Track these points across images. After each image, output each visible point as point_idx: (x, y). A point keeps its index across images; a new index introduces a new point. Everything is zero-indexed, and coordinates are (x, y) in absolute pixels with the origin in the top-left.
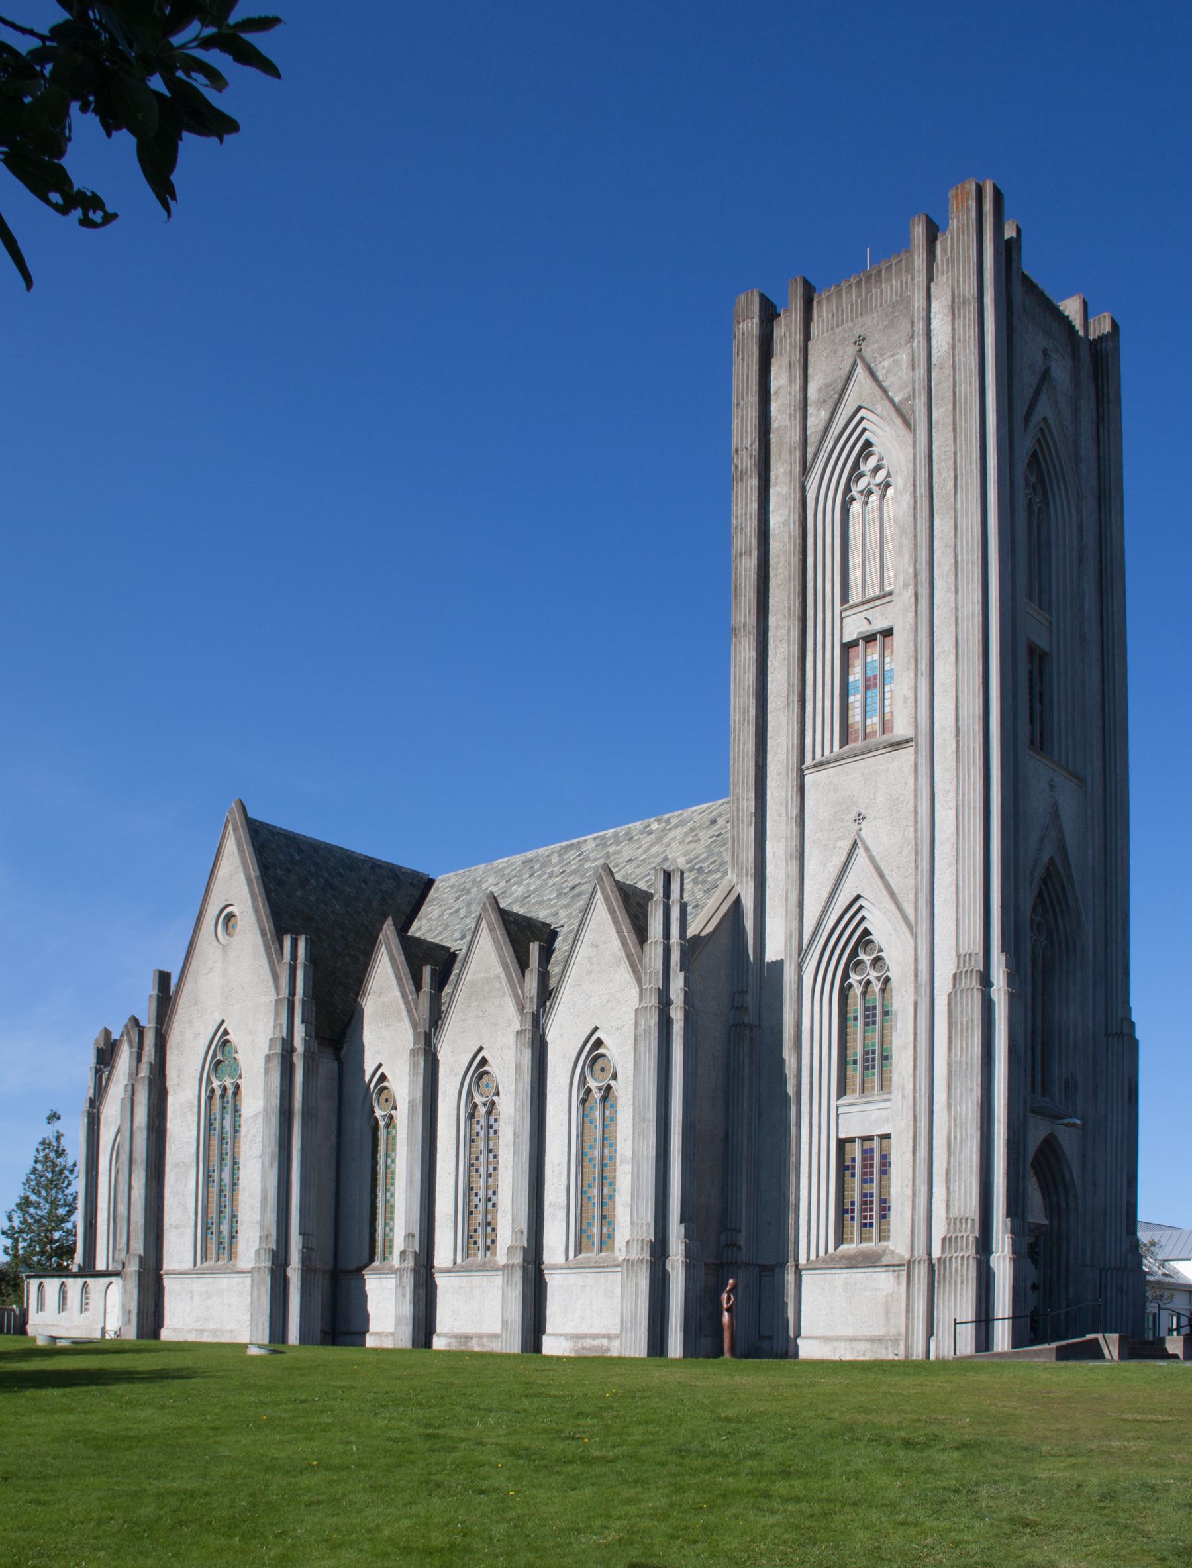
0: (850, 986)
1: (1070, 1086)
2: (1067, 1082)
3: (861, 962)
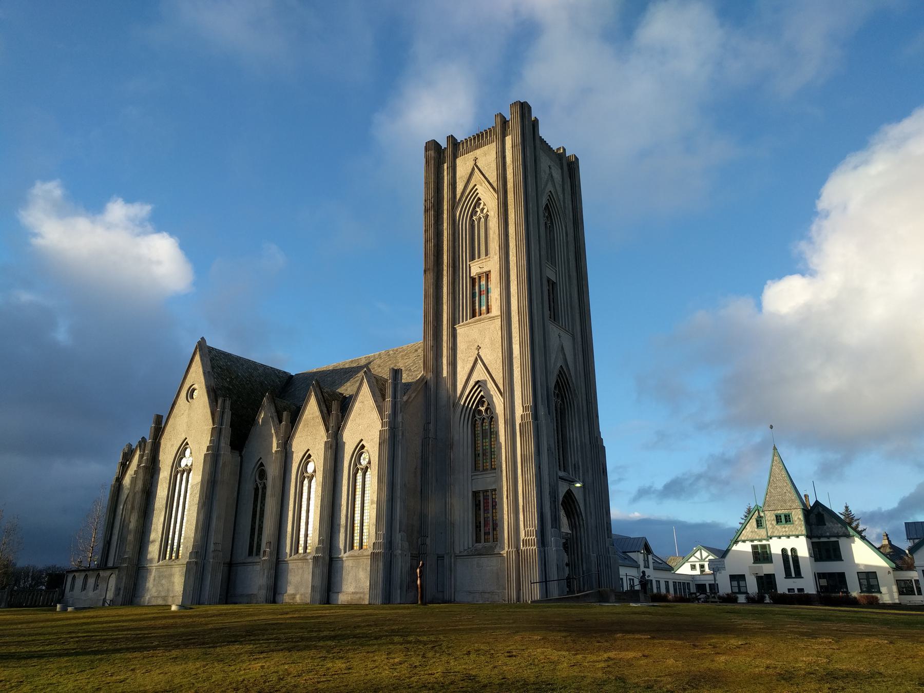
0: (476, 420)
1: (575, 467)
2: (575, 465)
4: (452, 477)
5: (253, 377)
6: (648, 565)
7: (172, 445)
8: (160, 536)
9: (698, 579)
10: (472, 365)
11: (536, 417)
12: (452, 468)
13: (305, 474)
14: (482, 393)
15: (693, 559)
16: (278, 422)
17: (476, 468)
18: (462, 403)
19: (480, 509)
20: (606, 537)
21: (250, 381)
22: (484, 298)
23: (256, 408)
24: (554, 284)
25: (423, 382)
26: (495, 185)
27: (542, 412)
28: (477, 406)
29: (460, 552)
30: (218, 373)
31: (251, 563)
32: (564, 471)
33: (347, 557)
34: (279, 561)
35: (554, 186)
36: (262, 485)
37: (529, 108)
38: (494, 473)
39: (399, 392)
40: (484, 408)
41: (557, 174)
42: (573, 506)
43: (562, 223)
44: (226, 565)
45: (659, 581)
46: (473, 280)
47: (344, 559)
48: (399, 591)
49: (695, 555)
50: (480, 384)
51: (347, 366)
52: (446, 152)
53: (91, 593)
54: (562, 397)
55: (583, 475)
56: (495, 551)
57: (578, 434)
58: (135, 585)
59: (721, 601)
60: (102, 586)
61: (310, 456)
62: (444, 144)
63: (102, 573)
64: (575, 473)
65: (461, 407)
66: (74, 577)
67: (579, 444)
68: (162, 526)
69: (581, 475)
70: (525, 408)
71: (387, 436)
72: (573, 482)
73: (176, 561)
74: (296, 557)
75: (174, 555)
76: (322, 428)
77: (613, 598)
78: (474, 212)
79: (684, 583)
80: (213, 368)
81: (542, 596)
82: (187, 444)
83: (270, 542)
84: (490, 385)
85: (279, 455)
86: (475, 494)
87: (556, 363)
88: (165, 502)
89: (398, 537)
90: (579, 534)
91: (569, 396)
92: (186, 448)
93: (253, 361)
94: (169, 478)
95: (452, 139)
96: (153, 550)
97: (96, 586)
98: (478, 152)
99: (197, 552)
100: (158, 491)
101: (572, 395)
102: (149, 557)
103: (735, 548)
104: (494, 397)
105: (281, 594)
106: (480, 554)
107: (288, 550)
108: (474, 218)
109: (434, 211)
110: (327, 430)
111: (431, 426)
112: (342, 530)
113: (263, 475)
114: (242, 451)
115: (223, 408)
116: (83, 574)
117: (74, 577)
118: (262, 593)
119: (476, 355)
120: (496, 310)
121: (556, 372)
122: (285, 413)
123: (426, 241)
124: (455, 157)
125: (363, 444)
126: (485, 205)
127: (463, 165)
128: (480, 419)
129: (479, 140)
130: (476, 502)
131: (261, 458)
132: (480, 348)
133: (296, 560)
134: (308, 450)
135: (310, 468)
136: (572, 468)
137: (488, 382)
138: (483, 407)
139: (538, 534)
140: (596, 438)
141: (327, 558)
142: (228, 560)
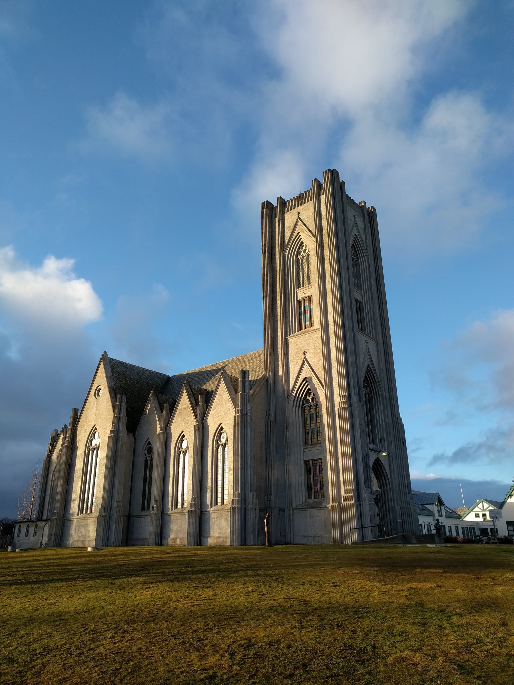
0: (305, 407)
1: (382, 441)
2: (381, 440)
3: (308, 400)
4: (288, 450)
5: (142, 379)
6: (441, 514)
7: (86, 430)
8: (79, 496)
9: (481, 525)
10: (300, 366)
11: (350, 404)
12: (288, 443)
13: (181, 450)
14: (309, 387)
15: (476, 509)
16: (160, 411)
17: (306, 443)
18: (294, 394)
19: (310, 474)
20: (407, 493)
21: (139, 382)
22: (308, 315)
23: (144, 401)
24: (360, 303)
25: (265, 380)
26: (314, 232)
27: (355, 399)
28: (306, 396)
29: (297, 506)
30: (116, 377)
31: (143, 515)
32: (373, 444)
33: (213, 511)
34: (163, 514)
35: (358, 231)
36: (150, 458)
37: (338, 174)
38: (320, 446)
39: (247, 387)
40: (311, 398)
41: (360, 222)
42: (380, 470)
43: (365, 257)
44: (126, 517)
45: (450, 527)
46: (299, 302)
47: (211, 512)
48: (252, 536)
49: (478, 506)
50: (307, 380)
51: (209, 369)
52: (277, 209)
53: (31, 538)
54: (370, 388)
55: (388, 446)
56: (323, 505)
57: (383, 416)
58: (62, 532)
59: (500, 542)
60: (39, 533)
61: (184, 436)
62: (275, 204)
63: (39, 524)
64: (382, 445)
65: (293, 398)
66: (20, 527)
67: (384, 423)
68: (79, 489)
69: (386, 447)
70: (341, 398)
71: (239, 420)
72: (380, 452)
73: (90, 514)
74: (176, 511)
75: (89, 510)
76: (192, 415)
77: (414, 540)
78: (299, 253)
79: (470, 528)
80: (113, 373)
81: (359, 539)
82: (96, 429)
83: (157, 500)
84: (315, 381)
85: (161, 436)
86: (306, 462)
87: (364, 362)
88: (81, 471)
89: (250, 495)
90: (386, 491)
91: (375, 387)
92: (95, 432)
93: (141, 368)
94: (84, 454)
95: (281, 200)
96: (74, 507)
97: (35, 534)
98: (301, 208)
99: (105, 508)
100: (76, 464)
101: (377, 386)
102: (71, 511)
103: (509, 500)
104: (318, 390)
105: (166, 538)
106: (311, 507)
107: (170, 506)
108: (299, 257)
109: (269, 253)
110: (196, 417)
111: (272, 412)
112: (209, 491)
113: (150, 451)
114: (135, 433)
115: (121, 402)
116: (26, 525)
117: (20, 527)
118: (152, 539)
119: (303, 358)
120: (317, 324)
121: (364, 369)
122: (165, 405)
123: (264, 275)
124: (283, 212)
125: (222, 427)
126: (306, 247)
127: (290, 219)
128: (308, 406)
129: (301, 199)
130: (307, 468)
131: (149, 438)
132: (306, 353)
133: (176, 513)
134: (183, 432)
135: (184, 445)
136: (379, 442)
137: (313, 378)
138: (310, 397)
139: (355, 492)
140: (396, 418)
141: (198, 511)
142: (127, 514)
